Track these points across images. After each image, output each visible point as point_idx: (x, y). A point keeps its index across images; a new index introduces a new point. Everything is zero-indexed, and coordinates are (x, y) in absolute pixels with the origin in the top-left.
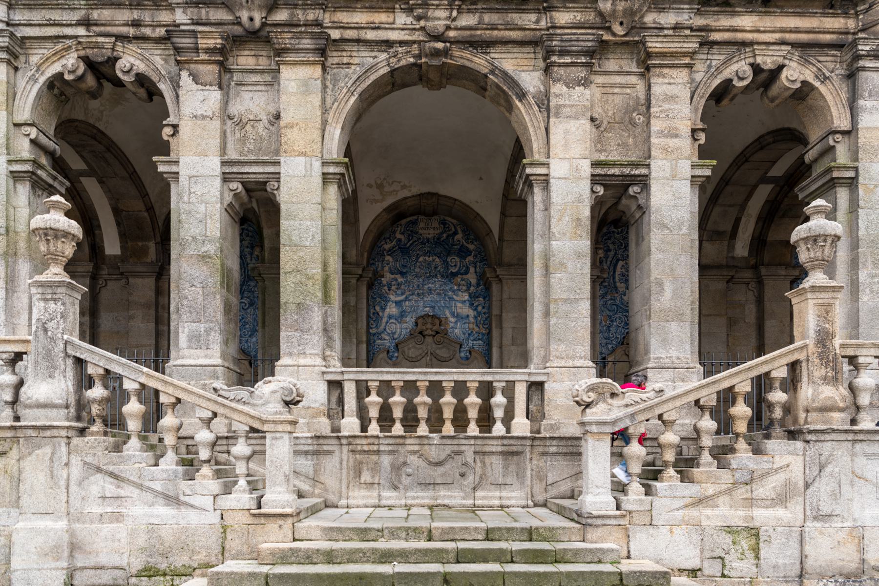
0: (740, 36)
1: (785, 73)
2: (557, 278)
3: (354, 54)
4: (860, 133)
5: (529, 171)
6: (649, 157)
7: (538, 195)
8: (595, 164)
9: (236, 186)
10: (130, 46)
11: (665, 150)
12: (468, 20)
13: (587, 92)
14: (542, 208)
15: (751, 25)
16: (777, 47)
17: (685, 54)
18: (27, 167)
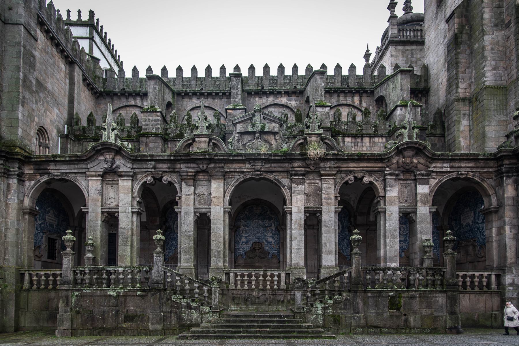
0: (350, 169)
1: (364, 180)
2: (294, 242)
4: (387, 198)
6: (322, 205)
7: (288, 217)
9: (198, 214)
10: (167, 174)
12: (268, 165)
13: (303, 186)
17: (332, 175)
18: (137, 210)
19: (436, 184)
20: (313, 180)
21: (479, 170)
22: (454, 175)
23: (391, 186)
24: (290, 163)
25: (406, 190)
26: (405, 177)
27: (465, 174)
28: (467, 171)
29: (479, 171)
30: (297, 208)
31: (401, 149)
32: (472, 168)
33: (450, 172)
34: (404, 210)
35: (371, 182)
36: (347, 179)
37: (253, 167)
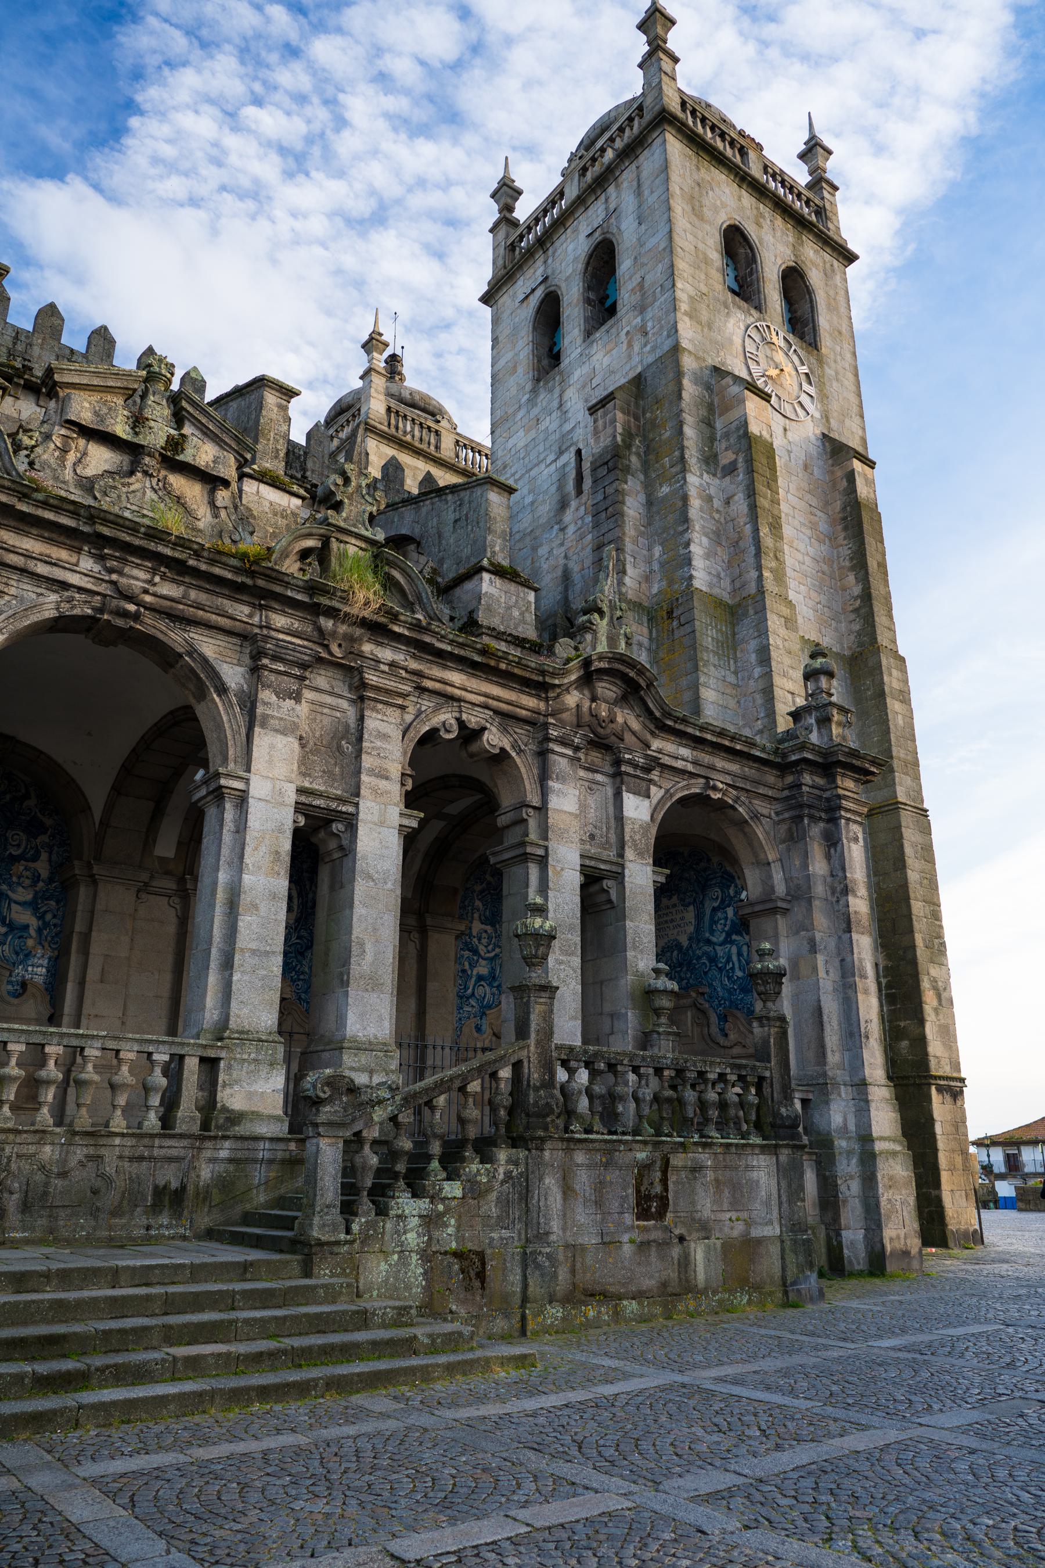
0: (449, 689)
3: (12, 582)
5: (223, 782)
6: (358, 795)
8: (300, 791)
11: (375, 791)
12: (168, 589)
14: (233, 829)
20: (331, 694)
23: (562, 779)
24: (261, 607)
25: (591, 801)
28: (726, 784)
29: (747, 791)
30: (269, 785)
33: (692, 775)
35: (502, 749)
37: (114, 577)
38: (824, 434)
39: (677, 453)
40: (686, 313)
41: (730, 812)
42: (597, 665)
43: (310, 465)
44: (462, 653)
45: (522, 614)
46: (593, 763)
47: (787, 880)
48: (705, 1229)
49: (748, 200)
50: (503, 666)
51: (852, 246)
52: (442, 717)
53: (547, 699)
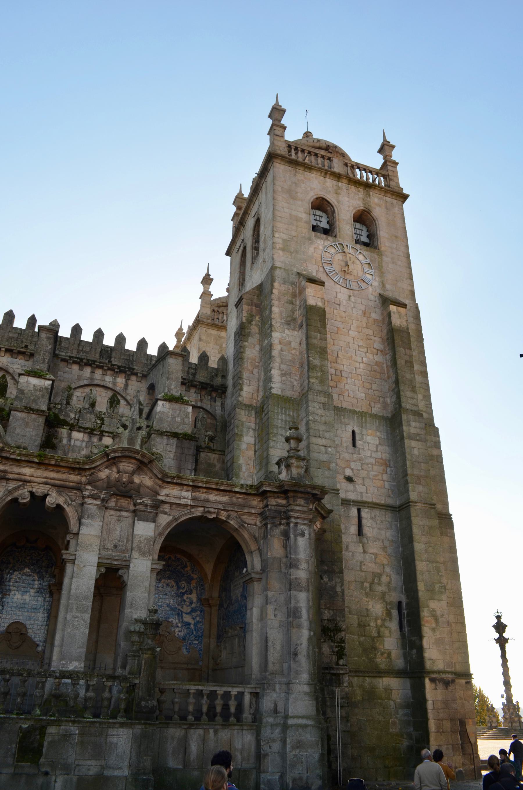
0: (23, 477)
1: (47, 500)
4: (80, 536)
15: (29, 473)
16: (44, 486)
19: (169, 524)
21: (236, 510)
22: (199, 512)
23: (91, 517)
26: (119, 505)
27: (214, 513)
28: (219, 509)
29: (236, 512)
31: (114, 458)
32: (225, 503)
33: (192, 506)
34: (109, 561)
35: (59, 506)
36: (16, 494)
38: (380, 294)
39: (269, 322)
40: (280, 249)
41: (227, 523)
42: (113, 455)
43: (113, 354)
44: (27, 459)
45: (183, 419)
46: (121, 506)
47: (262, 561)
48: (67, 769)
49: (330, 182)
50: (53, 462)
51: (405, 192)
52: (20, 492)
53: (86, 476)
